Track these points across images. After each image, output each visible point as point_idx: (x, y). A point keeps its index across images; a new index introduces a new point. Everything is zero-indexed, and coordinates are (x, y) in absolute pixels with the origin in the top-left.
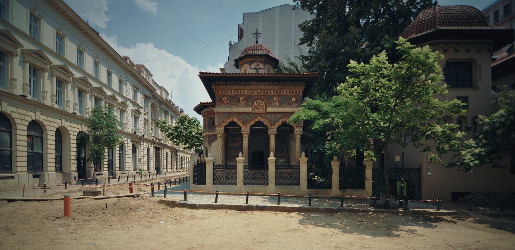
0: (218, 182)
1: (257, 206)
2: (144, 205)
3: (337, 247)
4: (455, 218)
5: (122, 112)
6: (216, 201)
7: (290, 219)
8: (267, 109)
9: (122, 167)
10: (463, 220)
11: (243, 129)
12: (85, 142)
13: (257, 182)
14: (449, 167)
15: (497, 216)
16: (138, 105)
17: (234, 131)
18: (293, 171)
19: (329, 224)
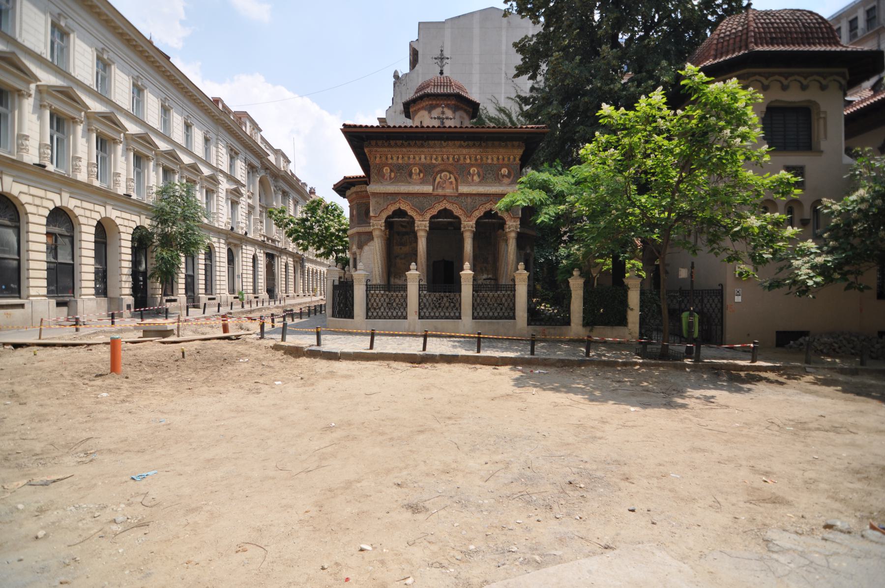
0: (375, 314)
1: (441, 355)
2: (248, 352)
5: (210, 193)
6: (371, 347)
7: (498, 377)
8: (460, 188)
11: (417, 223)
13: (442, 314)
14: (771, 287)
15: (854, 372)
16: (237, 182)
17: (402, 226)
18: (504, 295)
19: (565, 387)
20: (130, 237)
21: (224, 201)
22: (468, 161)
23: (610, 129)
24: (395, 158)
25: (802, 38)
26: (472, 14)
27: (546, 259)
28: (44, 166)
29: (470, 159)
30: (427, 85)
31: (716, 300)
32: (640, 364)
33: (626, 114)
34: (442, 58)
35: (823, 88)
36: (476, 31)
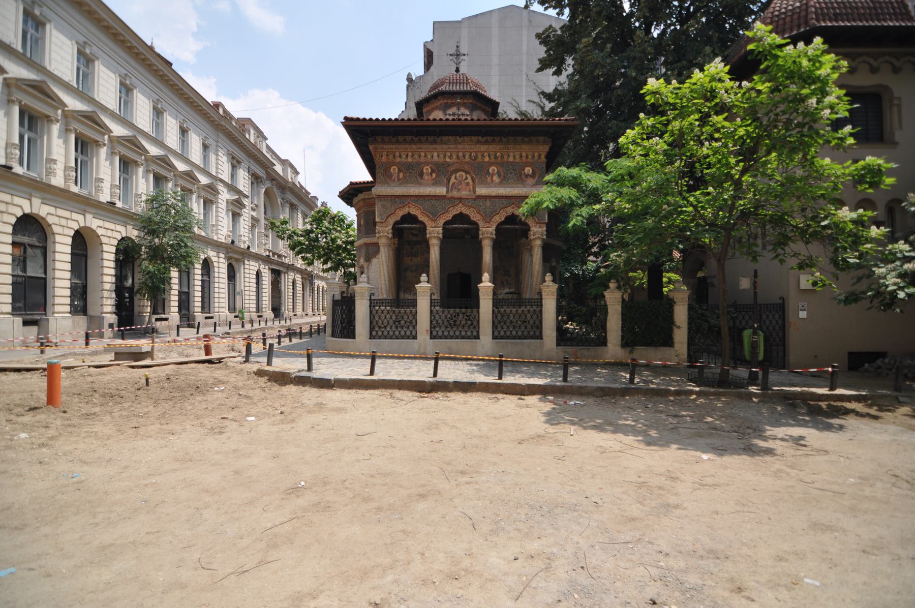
0: (380, 333)
2: (226, 379)
3: (641, 485)
4: (870, 406)
5: (208, 203)
6: (372, 373)
7: (524, 410)
8: (477, 189)
9: (206, 304)
10: (889, 411)
11: (429, 229)
12: (133, 257)
13: (457, 333)
16: (239, 192)
17: (413, 235)
19: (611, 424)
20: (113, 250)
21: (224, 212)
22: (487, 159)
23: (655, 110)
24: (404, 156)
25: (870, 14)
26: (490, 12)
27: (572, 273)
28: (11, 168)
29: (489, 156)
30: (442, 83)
31: (777, 316)
32: (696, 393)
33: (679, 88)
34: (458, 55)
35: (896, 70)
36: (495, 30)
